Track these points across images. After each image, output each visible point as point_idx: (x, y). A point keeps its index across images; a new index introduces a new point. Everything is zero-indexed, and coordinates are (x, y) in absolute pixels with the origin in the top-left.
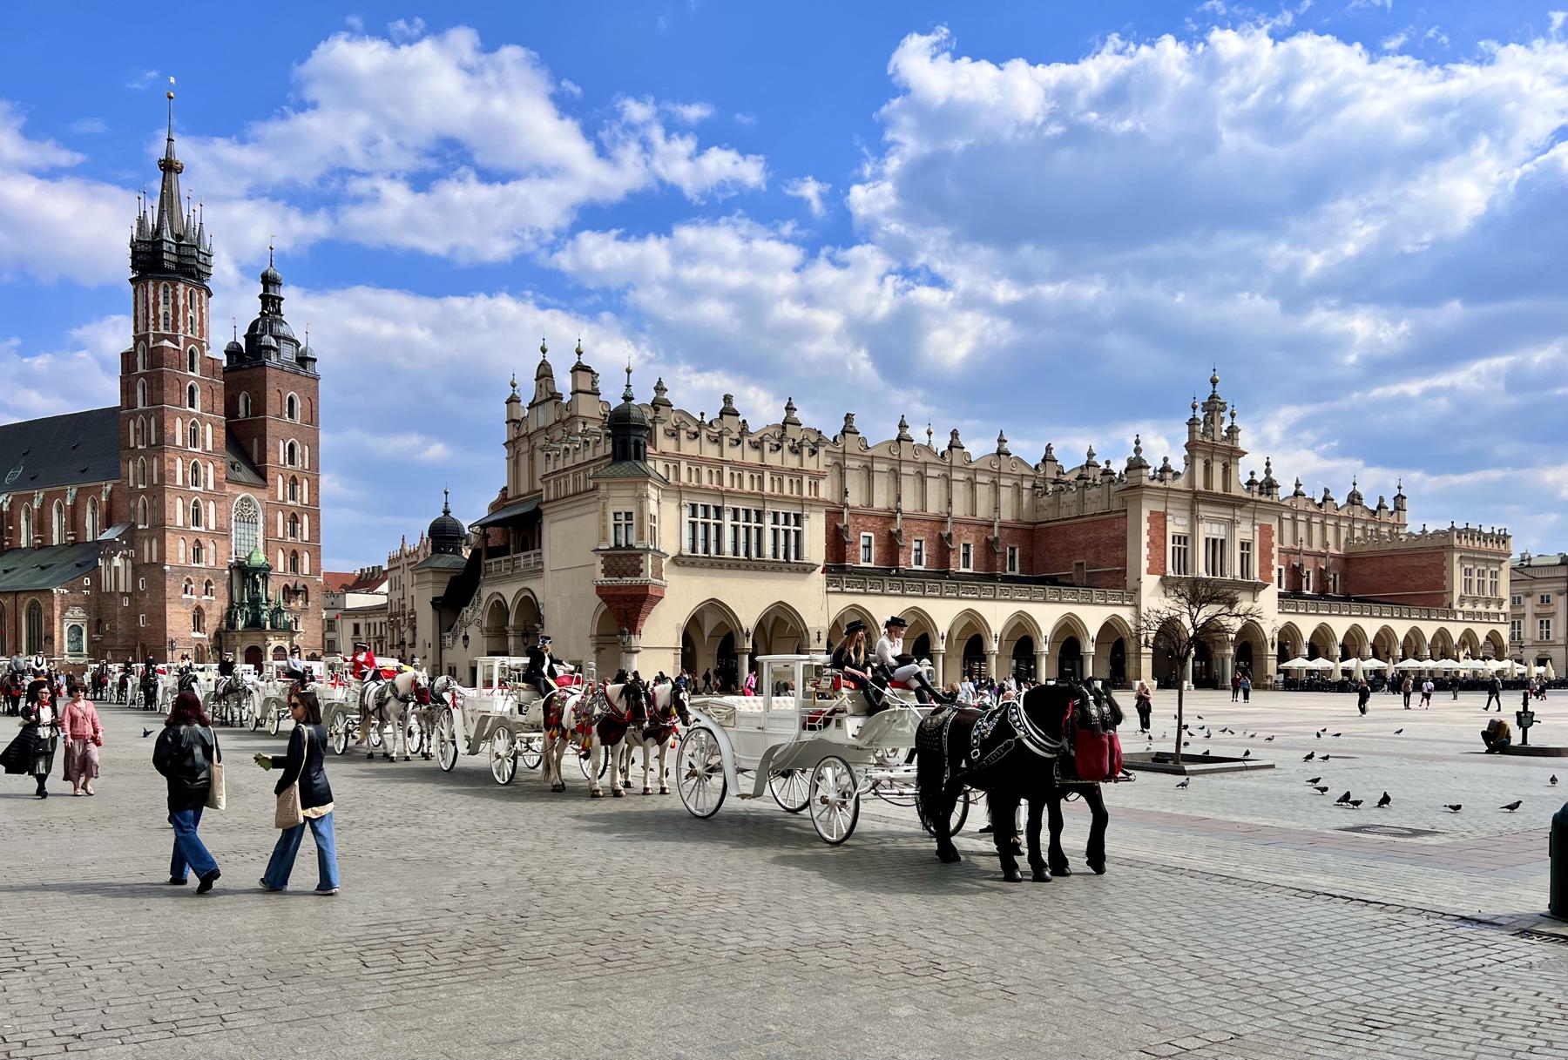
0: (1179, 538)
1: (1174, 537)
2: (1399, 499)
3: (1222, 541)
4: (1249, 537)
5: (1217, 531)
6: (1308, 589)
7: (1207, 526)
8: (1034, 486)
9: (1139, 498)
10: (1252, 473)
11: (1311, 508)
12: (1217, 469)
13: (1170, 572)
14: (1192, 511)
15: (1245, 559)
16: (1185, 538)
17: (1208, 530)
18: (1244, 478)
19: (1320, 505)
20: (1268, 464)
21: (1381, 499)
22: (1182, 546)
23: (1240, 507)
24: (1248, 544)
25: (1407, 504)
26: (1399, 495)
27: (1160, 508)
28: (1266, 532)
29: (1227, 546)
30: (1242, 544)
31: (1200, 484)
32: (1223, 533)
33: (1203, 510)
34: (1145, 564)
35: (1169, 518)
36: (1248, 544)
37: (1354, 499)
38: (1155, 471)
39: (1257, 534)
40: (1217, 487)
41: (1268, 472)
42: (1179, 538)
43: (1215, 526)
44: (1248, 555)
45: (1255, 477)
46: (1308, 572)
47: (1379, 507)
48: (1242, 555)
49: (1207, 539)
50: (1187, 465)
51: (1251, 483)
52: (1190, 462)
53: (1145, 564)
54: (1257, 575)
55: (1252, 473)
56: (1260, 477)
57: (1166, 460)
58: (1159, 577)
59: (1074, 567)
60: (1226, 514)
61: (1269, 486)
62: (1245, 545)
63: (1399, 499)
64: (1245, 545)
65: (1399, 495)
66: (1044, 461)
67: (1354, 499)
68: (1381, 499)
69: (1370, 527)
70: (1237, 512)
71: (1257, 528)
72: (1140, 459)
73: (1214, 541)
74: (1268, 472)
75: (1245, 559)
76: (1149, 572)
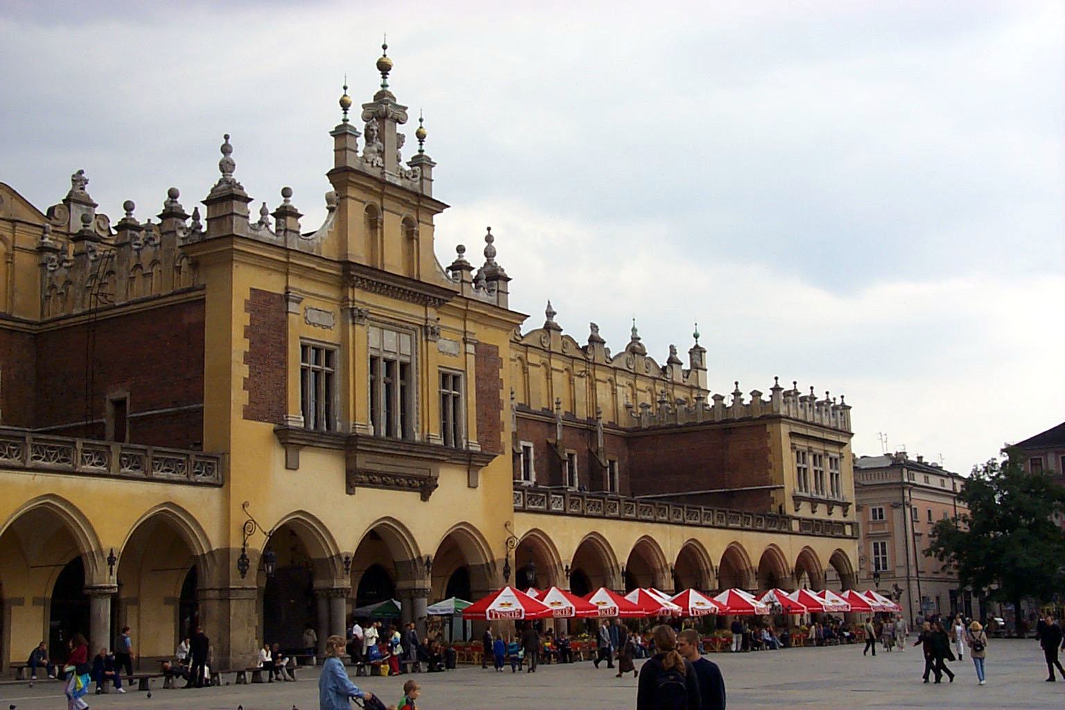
0: (318, 350)
1: (304, 348)
2: (697, 352)
3: (404, 366)
4: (455, 364)
5: (393, 344)
6: (572, 484)
7: (374, 333)
8: (42, 249)
9: (227, 260)
10: (461, 249)
11: (571, 351)
12: (392, 225)
13: (295, 418)
14: (344, 300)
15: (449, 404)
16: (329, 353)
17: (374, 342)
18: (446, 258)
19: (585, 348)
20: (489, 239)
21: (673, 350)
22: (322, 366)
23: (442, 303)
24: (456, 378)
25: (708, 360)
26: (697, 346)
27: (273, 284)
28: (487, 356)
29: (415, 376)
30: (445, 377)
31: (358, 252)
32: (406, 350)
33: (362, 298)
34: (239, 397)
35: (292, 307)
36: (456, 378)
37: (635, 349)
38: (263, 212)
39: (471, 360)
40: (394, 262)
41: (489, 253)
42: (318, 350)
43: (390, 339)
44: (456, 398)
45: (466, 257)
46: (571, 456)
47: (672, 361)
48: (445, 397)
49: (373, 360)
50: (331, 210)
51: (460, 266)
52: (336, 205)
53: (239, 397)
54: (473, 440)
55: (461, 249)
56: (476, 260)
57: (286, 193)
58: (272, 426)
59: (109, 408)
60: (413, 312)
61: (494, 277)
62: (449, 379)
63: (697, 352)
64: (449, 379)
65: (697, 346)
66: (67, 201)
67: (635, 349)
68: (673, 350)
69: (659, 388)
70: (432, 313)
71: (471, 348)
72: (233, 184)
73: (390, 364)
74: (489, 253)
75: (449, 404)
76: (249, 414)
